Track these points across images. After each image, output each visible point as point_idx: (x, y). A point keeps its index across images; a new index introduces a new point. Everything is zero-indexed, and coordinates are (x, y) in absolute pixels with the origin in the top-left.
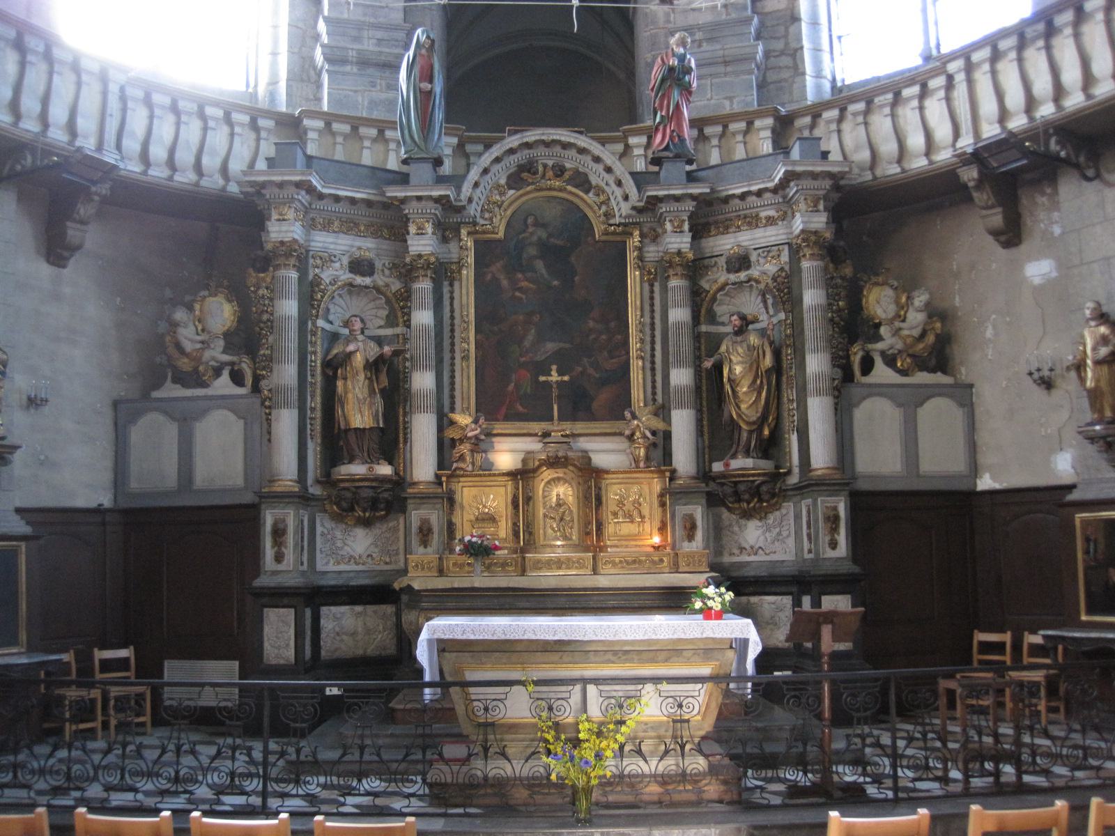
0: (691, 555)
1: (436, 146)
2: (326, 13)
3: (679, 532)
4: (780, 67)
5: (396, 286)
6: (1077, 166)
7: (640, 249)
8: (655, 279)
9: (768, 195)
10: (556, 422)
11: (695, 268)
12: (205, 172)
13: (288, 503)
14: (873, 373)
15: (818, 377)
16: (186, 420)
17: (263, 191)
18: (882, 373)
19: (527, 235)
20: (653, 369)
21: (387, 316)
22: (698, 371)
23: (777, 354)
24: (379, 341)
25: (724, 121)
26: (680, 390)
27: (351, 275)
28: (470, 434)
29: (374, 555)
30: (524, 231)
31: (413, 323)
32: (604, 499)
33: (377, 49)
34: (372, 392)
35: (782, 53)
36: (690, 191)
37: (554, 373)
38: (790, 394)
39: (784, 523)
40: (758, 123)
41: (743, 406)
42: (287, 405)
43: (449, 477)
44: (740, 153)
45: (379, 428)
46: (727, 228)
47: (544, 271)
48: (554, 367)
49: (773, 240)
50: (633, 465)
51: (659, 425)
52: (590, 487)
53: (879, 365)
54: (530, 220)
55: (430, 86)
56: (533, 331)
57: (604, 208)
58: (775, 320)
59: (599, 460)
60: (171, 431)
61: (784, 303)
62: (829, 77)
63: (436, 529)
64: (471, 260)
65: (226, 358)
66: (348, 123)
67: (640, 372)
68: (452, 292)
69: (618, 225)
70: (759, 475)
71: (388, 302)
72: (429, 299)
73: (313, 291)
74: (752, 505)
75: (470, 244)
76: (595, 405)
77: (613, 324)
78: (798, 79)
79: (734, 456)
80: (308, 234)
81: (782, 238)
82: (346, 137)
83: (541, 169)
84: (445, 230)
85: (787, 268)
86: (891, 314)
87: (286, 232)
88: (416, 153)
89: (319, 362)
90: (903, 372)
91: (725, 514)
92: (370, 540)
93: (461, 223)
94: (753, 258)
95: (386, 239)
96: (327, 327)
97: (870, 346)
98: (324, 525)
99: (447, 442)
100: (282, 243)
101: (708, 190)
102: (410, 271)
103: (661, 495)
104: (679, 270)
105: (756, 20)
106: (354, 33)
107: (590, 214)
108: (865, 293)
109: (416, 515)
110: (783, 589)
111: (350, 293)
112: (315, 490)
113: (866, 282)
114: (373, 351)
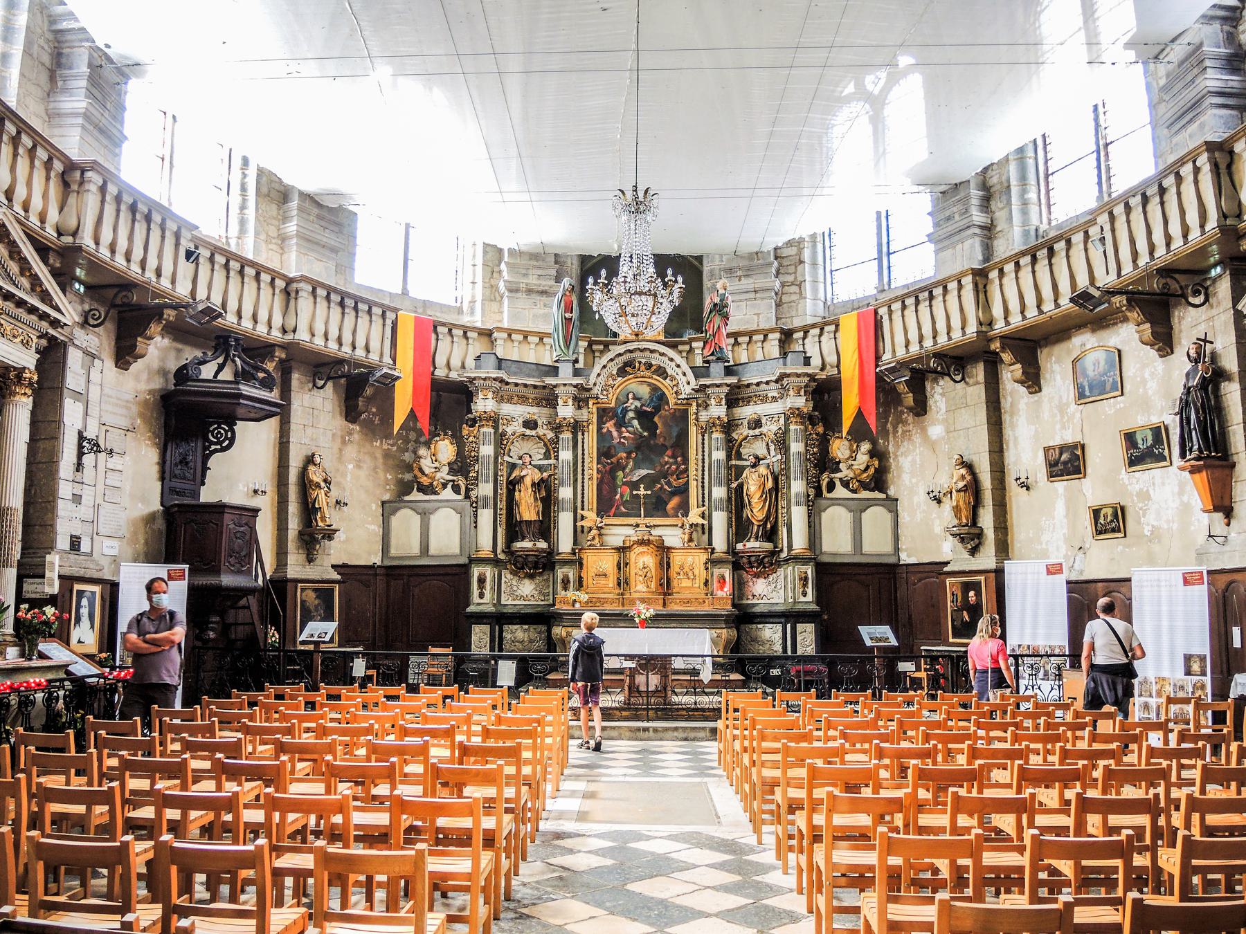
0: (722, 598)
2: (506, 259)
6: (949, 375)
7: (696, 414)
8: (705, 432)
9: (773, 385)
11: (729, 427)
15: (797, 495)
16: (425, 515)
18: (840, 492)
20: (703, 487)
22: (729, 489)
23: (776, 480)
24: (540, 468)
25: (750, 334)
26: (718, 500)
31: (560, 458)
34: (536, 499)
35: (793, 284)
38: (782, 503)
40: (770, 336)
42: (487, 506)
43: (580, 550)
44: (759, 356)
46: (749, 402)
48: (642, 486)
52: (663, 558)
57: (675, 389)
58: (774, 459)
60: (417, 519)
62: (823, 299)
63: (572, 581)
64: (595, 420)
68: (583, 439)
71: (545, 445)
75: (595, 410)
77: (679, 459)
79: (749, 540)
83: (637, 365)
90: (854, 491)
91: (745, 575)
92: (533, 586)
94: (763, 421)
97: (833, 475)
98: (507, 576)
99: (579, 529)
103: (706, 563)
104: (719, 428)
105: (776, 263)
106: (524, 272)
109: (560, 572)
110: (777, 620)
111: (523, 439)
112: (501, 556)
114: (537, 476)
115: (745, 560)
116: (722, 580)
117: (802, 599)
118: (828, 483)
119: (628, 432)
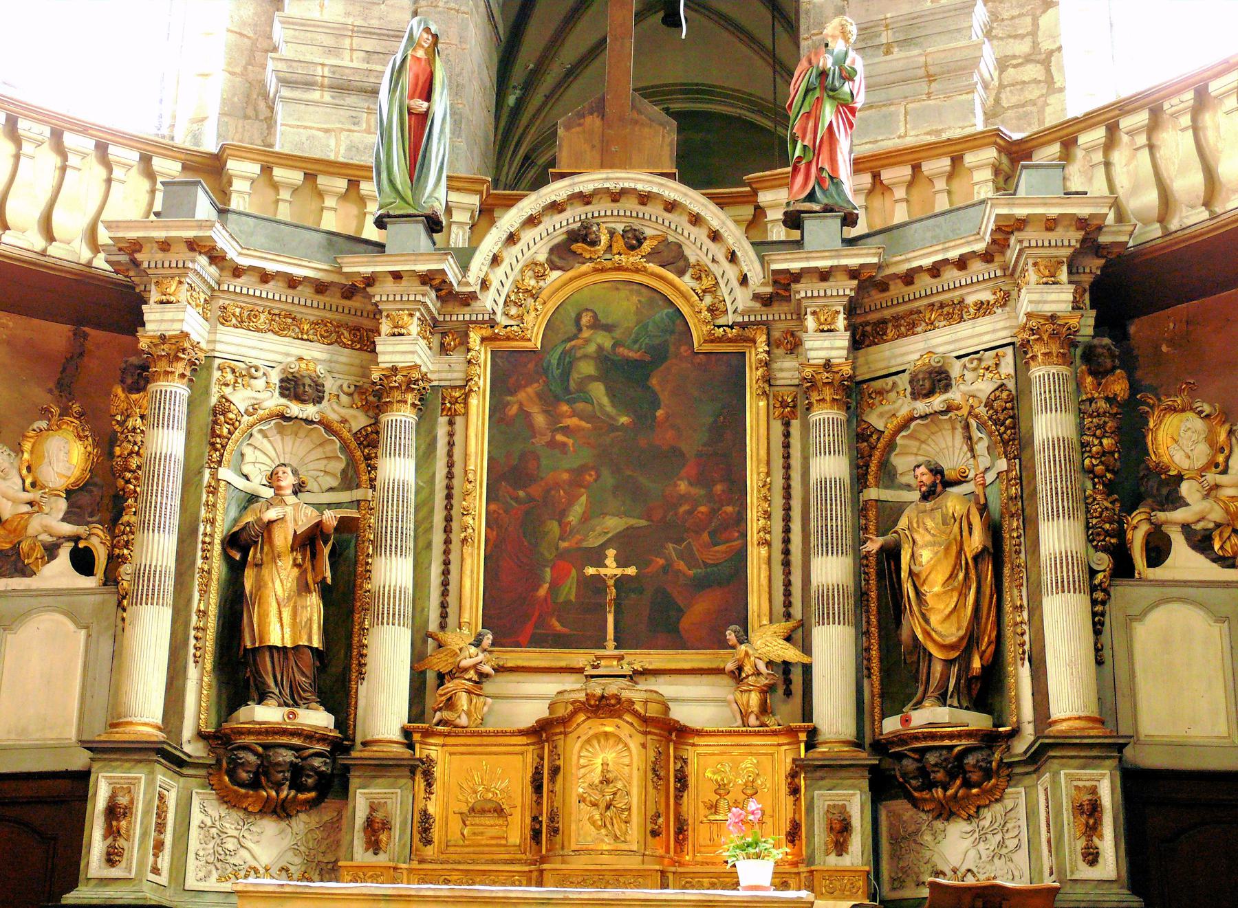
0: (840, 873)
1: (430, 196)
3: (821, 836)
4: (1024, 82)
5: (359, 421)
7: (767, 364)
8: (793, 414)
9: (977, 266)
10: (611, 643)
12: (57, 232)
13: (140, 761)
14: (1168, 562)
15: (1058, 561)
17: (138, 256)
19: (580, 342)
20: (786, 564)
21: (344, 472)
22: (861, 562)
23: (995, 531)
25: (914, 158)
26: (826, 595)
27: (284, 401)
28: (466, 663)
29: (292, 869)
30: (575, 337)
32: (691, 781)
33: (365, 66)
34: (303, 588)
35: (1028, 59)
36: (844, 262)
37: (610, 561)
38: (1014, 595)
39: (1009, 826)
40: (970, 159)
41: (934, 619)
45: (311, 648)
47: (605, 401)
48: (611, 553)
49: (988, 340)
50: (739, 722)
51: (792, 654)
53: (1180, 547)
54: (585, 320)
55: (425, 105)
56: (584, 499)
57: (708, 300)
59: (682, 714)
61: (1005, 443)
65: (68, 529)
66: (300, 168)
67: (764, 567)
68: (451, 435)
69: (732, 327)
70: (959, 736)
71: (345, 447)
72: (410, 440)
73: (215, 422)
74: (950, 792)
76: (685, 623)
77: (719, 488)
78: (1052, 100)
79: (918, 705)
80: (213, 331)
81: (1003, 336)
82: (295, 190)
83: (604, 239)
84: (444, 334)
85: (1011, 385)
86: (1199, 464)
87: (173, 321)
88: (396, 208)
89: (217, 541)
92: (287, 841)
93: (471, 322)
94: (955, 370)
95: (345, 346)
96: (240, 483)
97: (1162, 516)
99: (431, 677)
100: (163, 338)
101: (875, 260)
102: (378, 394)
103: (793, 775)
104: (828, 393)
106: (329, 41)
107: (685, 310)
108: (1151, 425)
109: (361, 800)
111: (281, 430)
112: (192, 748)
113: (1152, 407)
115: (909, 765)
116: (841, 830)
117: (1086, 872)
118: (1149, 537)
119: (574, 414)
